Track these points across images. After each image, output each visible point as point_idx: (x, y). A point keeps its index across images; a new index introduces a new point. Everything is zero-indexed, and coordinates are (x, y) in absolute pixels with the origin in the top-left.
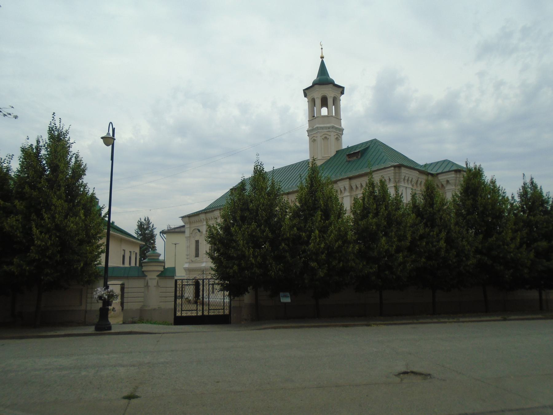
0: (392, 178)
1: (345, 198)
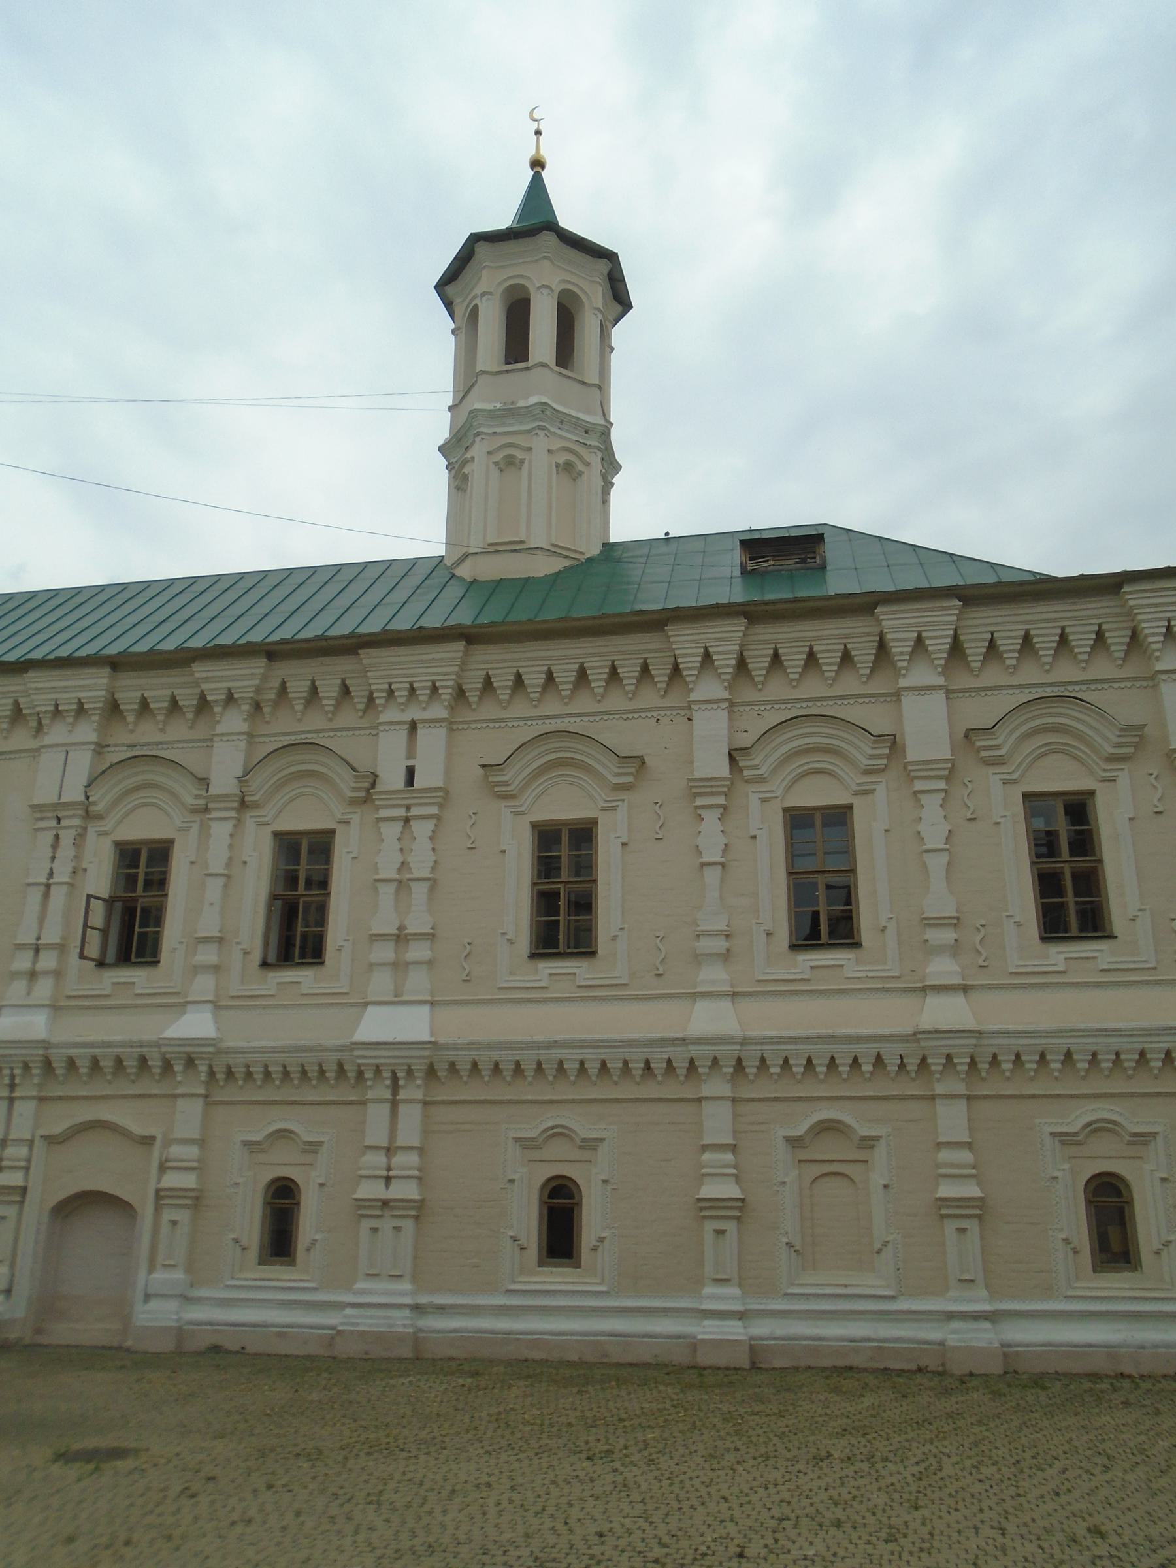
1: (907, 701)
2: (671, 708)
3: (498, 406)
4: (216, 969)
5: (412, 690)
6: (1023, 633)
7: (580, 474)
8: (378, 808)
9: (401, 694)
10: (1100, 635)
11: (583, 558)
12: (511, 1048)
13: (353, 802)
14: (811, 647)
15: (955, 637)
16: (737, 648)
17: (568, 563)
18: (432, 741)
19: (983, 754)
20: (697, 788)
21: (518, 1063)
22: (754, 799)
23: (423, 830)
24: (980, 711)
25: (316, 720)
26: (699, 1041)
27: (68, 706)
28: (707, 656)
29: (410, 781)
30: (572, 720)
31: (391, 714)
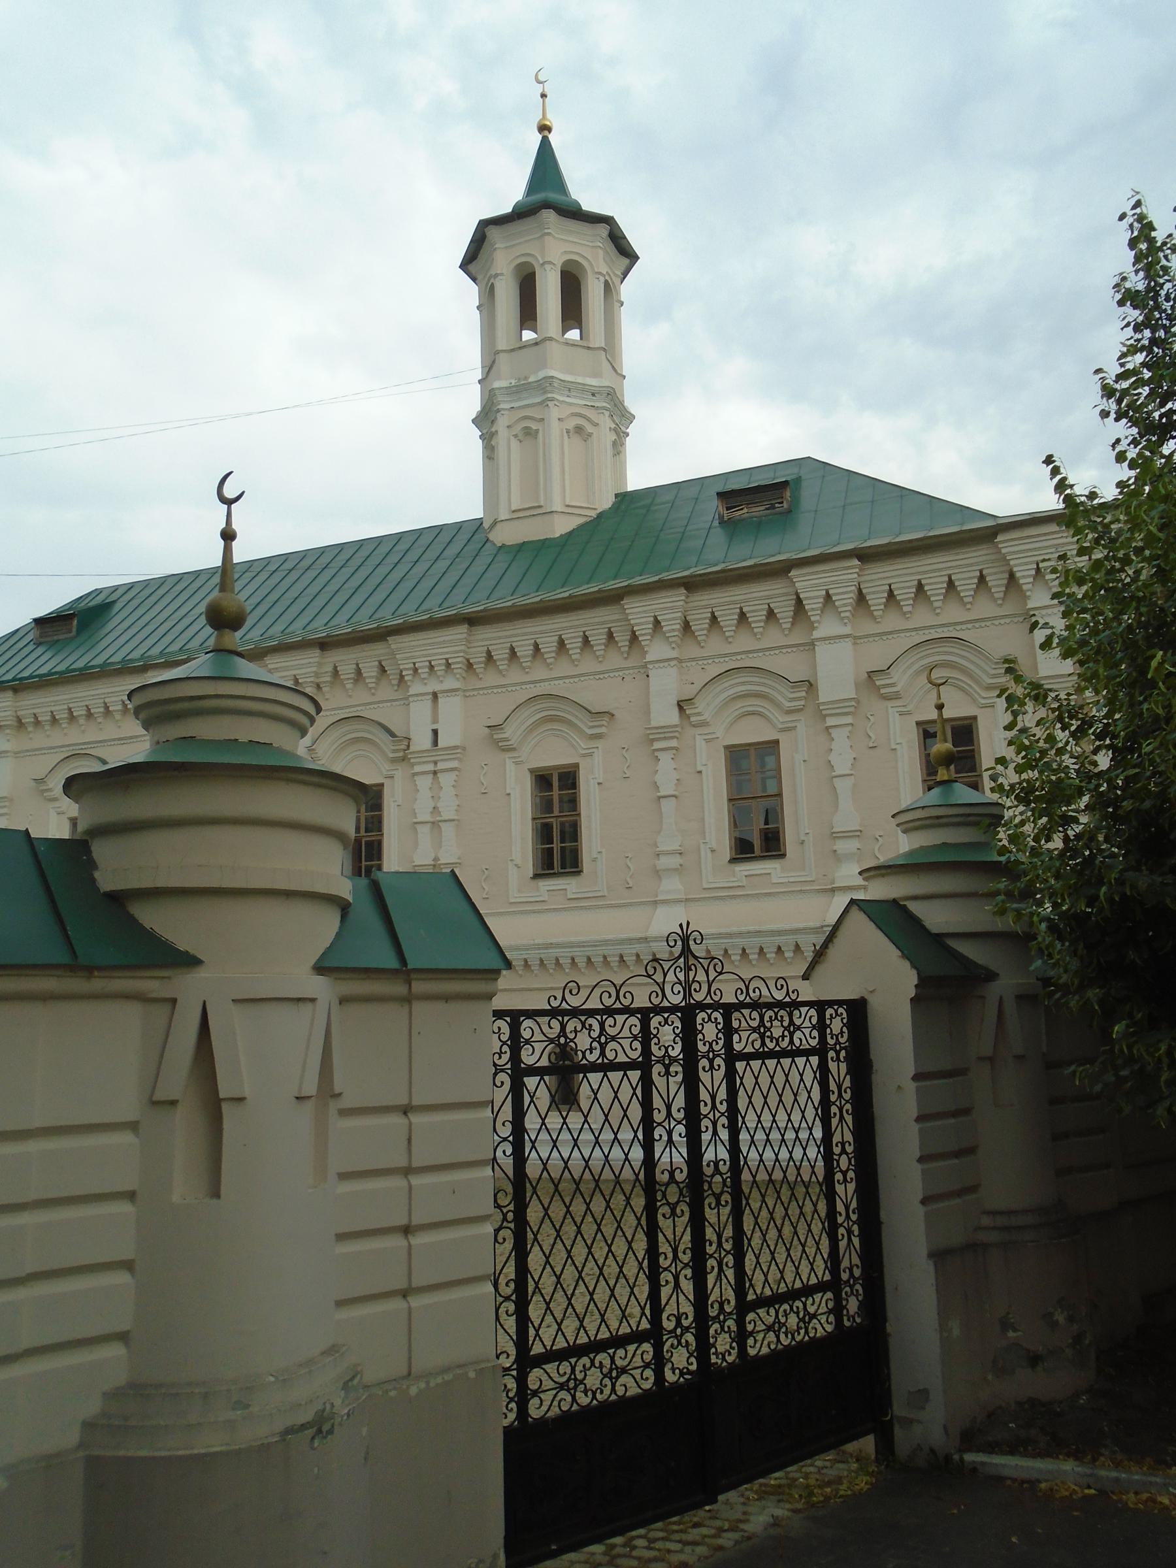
1: (820, 649)
2: (633, 668)
3: (513, 382)
5: (431, 667)
6: (916, 583)
7: (590, 435)
8: (413, 765)
9: (423, 671)
10: (982, 579)
11: (594, 514)
12: (519, 949)
13: (394, 761)
14: (741, 608)
15: (860, 591)
16: (679, 614)
17: (581, 520)
18: (451, 707)
19: (883, 691)
21: (526, 961)
22: (700, 743)
23: (446, 780)
24: (877, 655)
28: (657, 623)
29: (435, 742)
30: (556, 682)
31: (416, 688)
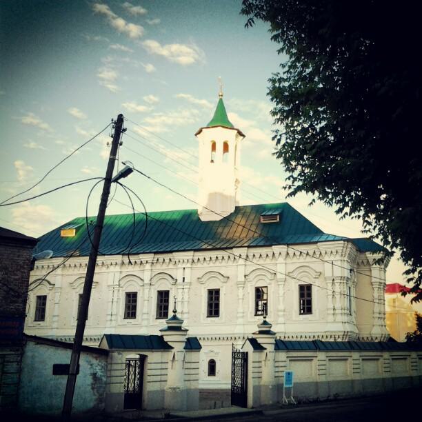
0: (340, 251)
1: (278, 265)
4: (147, 319)
20: (238, 283)
23: (186, 290)
24: (291, 268)
25: (164, 266)
26: (237, 334)
27: (114, 263)
31: (180, 266)
